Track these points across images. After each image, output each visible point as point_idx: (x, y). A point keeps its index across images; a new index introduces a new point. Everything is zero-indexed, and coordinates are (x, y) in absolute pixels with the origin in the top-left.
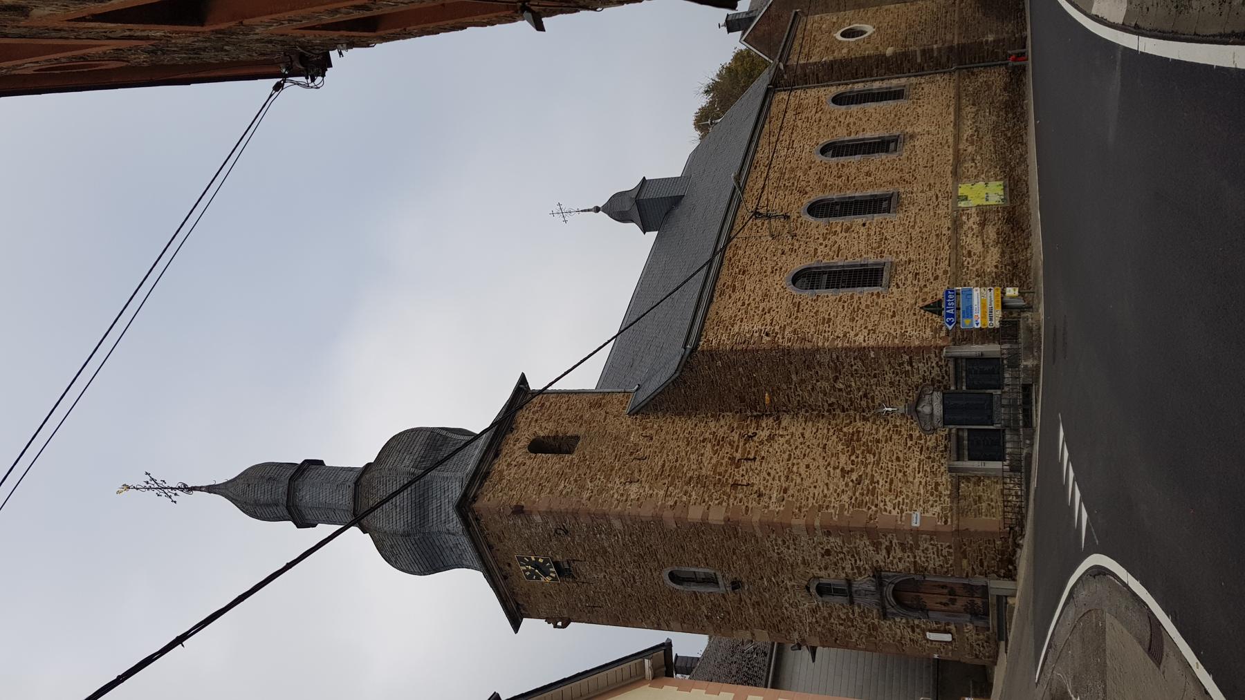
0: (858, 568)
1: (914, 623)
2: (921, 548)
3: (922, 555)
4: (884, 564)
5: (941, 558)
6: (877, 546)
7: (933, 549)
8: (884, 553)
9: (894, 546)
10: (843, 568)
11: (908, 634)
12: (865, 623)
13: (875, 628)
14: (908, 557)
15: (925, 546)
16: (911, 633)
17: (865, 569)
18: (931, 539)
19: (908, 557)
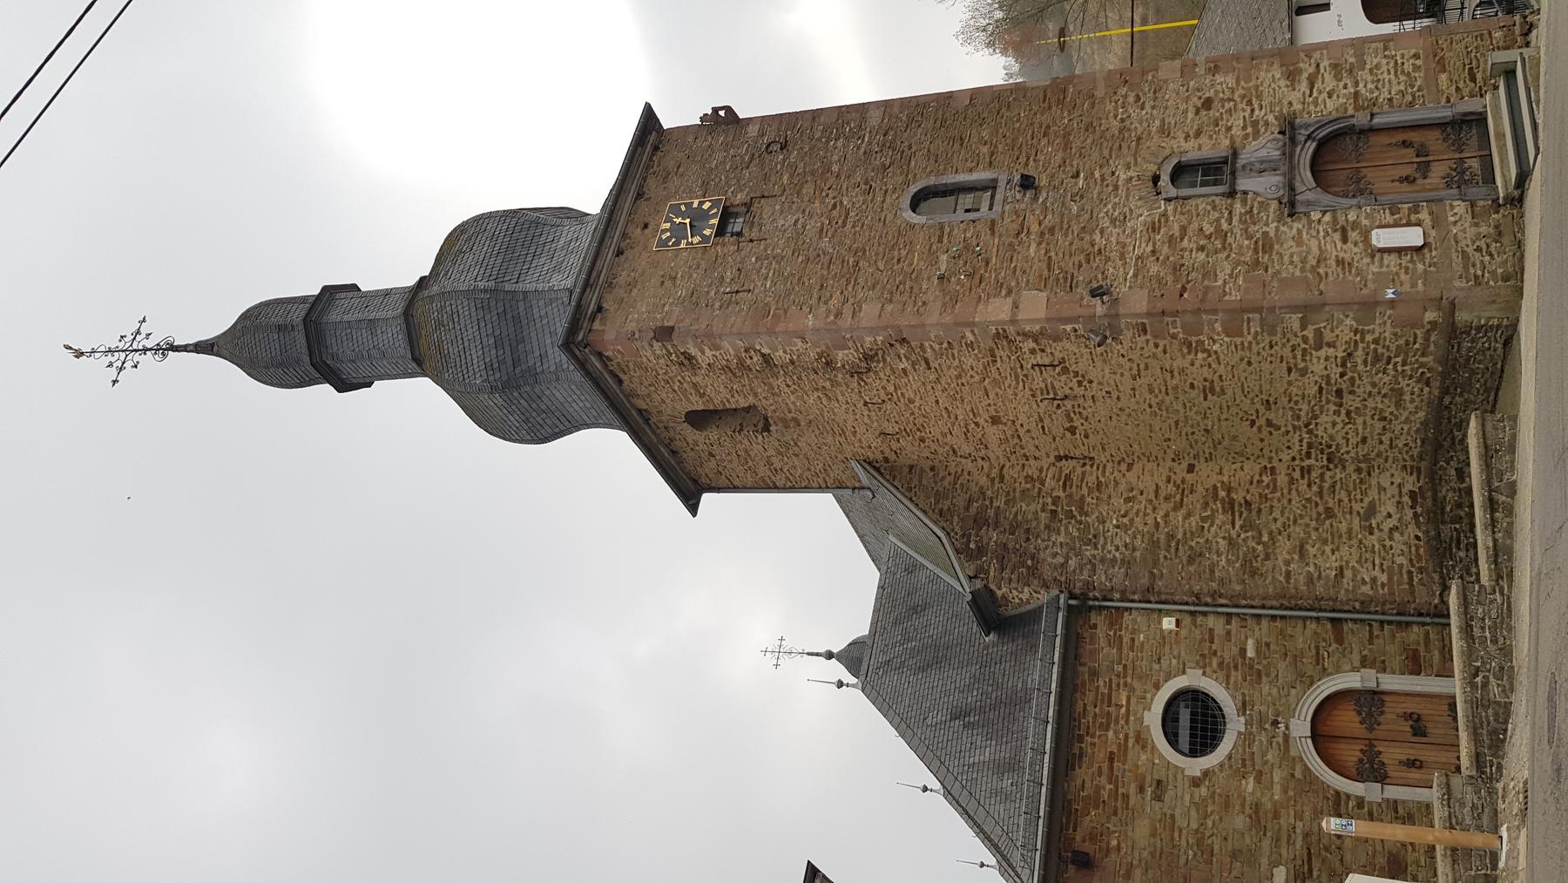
0: (1255, 124)
1: (1347, 220)
2: (1368, 67)
3: (1369, 78)
4: (1300, 107)
5: (1402, 78)
6: (1292, 76)
7: (1388, 63)
8: (1304, 86)
9: (1322, 71)
10: (1229, 129)
11: (1335, 248)
12: (1250, 237)
13: (1267, 245)
14: (1345, 87)
15: (1375, 61)
16: (1339, 245)
17: (1267, 124)
18: (1386, 49)
19: (1345, 87)
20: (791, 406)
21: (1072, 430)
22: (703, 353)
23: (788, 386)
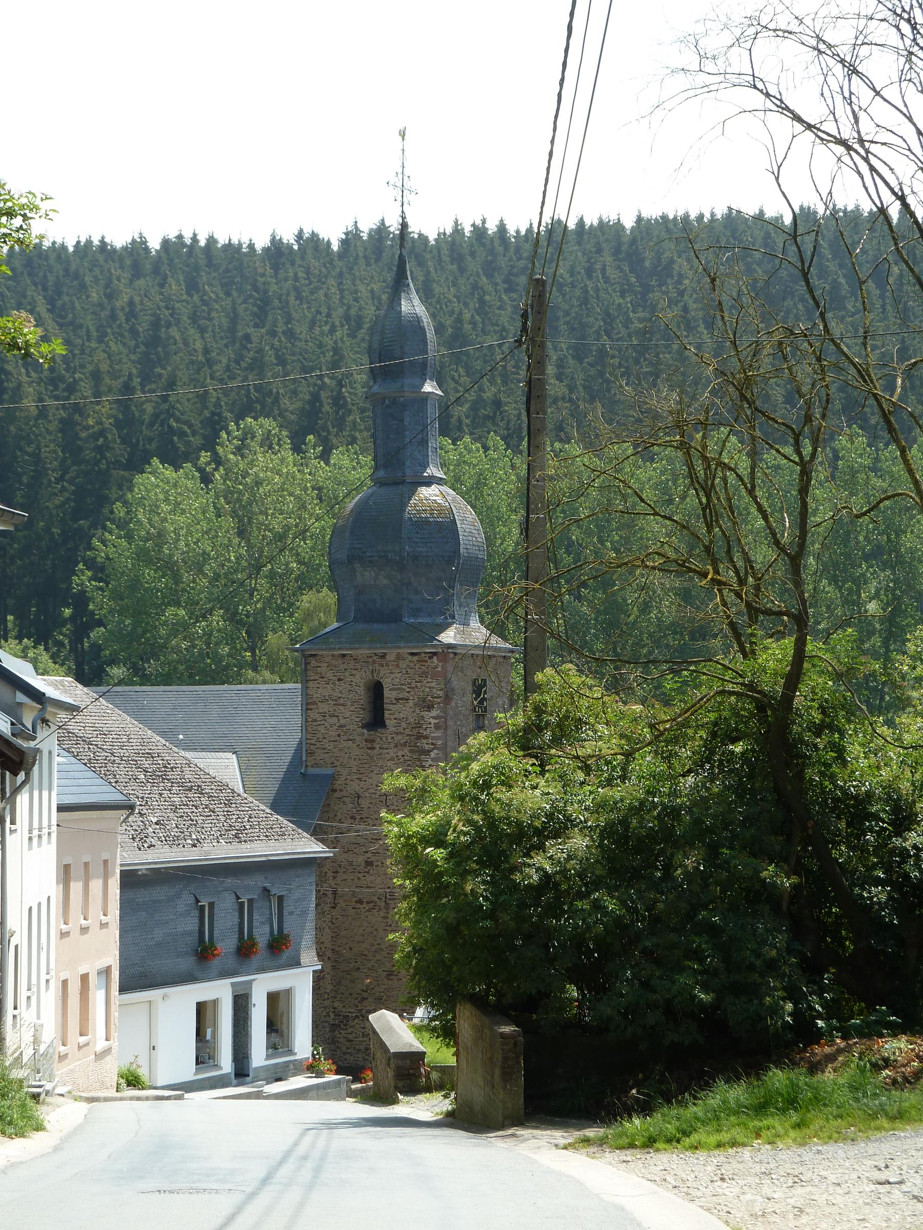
20: (386, 751)
21: (360, 902)
22: (433, 718)
23: (403, 756)
